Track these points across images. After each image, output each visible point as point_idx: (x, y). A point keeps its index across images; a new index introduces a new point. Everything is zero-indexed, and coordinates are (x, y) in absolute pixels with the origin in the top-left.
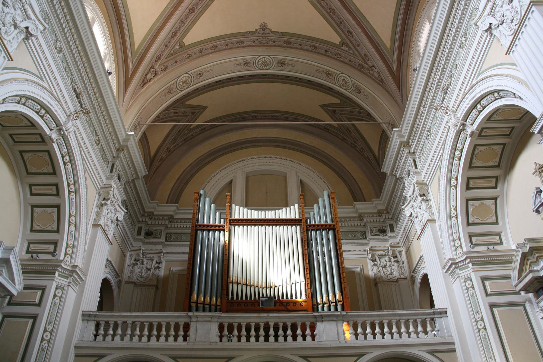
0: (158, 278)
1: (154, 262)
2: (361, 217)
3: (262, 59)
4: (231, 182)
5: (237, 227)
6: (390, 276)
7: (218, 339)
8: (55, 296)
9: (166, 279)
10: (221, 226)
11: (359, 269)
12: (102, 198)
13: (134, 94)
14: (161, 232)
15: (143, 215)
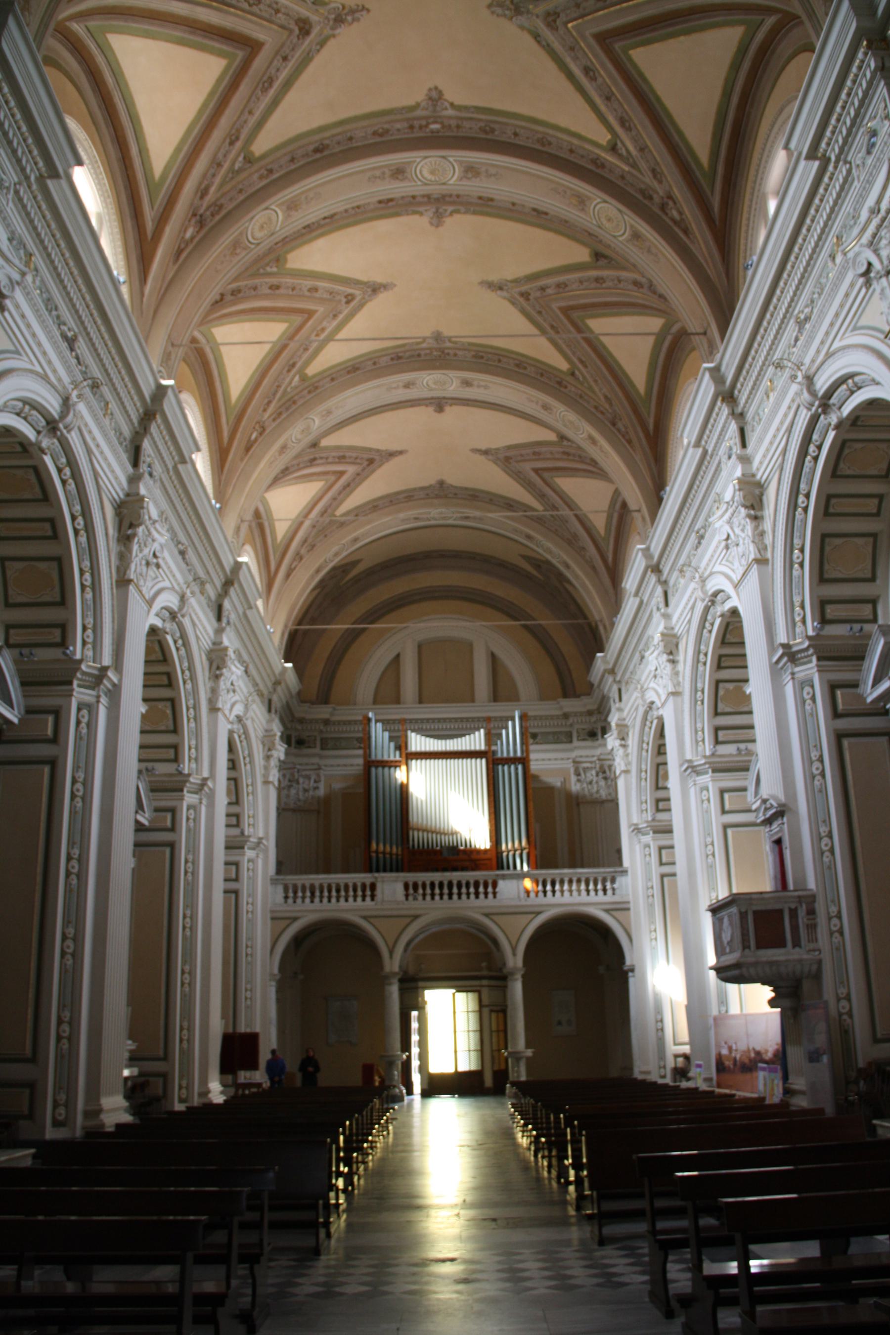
0: (319, 798)
1: (312, 781)
2: (566, 716)
3: (436, 513)
4: (398, 655)
5: (414, 761)
6: (595, 796)
7: (404, 898)
8: (248, 869)
9: (327, 801)
10: (396, 762)
11: (559, 784)
12: (266, 748)
13: (279, 593)
14: (315, 740)
15: (292, 721)
